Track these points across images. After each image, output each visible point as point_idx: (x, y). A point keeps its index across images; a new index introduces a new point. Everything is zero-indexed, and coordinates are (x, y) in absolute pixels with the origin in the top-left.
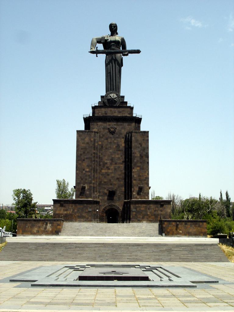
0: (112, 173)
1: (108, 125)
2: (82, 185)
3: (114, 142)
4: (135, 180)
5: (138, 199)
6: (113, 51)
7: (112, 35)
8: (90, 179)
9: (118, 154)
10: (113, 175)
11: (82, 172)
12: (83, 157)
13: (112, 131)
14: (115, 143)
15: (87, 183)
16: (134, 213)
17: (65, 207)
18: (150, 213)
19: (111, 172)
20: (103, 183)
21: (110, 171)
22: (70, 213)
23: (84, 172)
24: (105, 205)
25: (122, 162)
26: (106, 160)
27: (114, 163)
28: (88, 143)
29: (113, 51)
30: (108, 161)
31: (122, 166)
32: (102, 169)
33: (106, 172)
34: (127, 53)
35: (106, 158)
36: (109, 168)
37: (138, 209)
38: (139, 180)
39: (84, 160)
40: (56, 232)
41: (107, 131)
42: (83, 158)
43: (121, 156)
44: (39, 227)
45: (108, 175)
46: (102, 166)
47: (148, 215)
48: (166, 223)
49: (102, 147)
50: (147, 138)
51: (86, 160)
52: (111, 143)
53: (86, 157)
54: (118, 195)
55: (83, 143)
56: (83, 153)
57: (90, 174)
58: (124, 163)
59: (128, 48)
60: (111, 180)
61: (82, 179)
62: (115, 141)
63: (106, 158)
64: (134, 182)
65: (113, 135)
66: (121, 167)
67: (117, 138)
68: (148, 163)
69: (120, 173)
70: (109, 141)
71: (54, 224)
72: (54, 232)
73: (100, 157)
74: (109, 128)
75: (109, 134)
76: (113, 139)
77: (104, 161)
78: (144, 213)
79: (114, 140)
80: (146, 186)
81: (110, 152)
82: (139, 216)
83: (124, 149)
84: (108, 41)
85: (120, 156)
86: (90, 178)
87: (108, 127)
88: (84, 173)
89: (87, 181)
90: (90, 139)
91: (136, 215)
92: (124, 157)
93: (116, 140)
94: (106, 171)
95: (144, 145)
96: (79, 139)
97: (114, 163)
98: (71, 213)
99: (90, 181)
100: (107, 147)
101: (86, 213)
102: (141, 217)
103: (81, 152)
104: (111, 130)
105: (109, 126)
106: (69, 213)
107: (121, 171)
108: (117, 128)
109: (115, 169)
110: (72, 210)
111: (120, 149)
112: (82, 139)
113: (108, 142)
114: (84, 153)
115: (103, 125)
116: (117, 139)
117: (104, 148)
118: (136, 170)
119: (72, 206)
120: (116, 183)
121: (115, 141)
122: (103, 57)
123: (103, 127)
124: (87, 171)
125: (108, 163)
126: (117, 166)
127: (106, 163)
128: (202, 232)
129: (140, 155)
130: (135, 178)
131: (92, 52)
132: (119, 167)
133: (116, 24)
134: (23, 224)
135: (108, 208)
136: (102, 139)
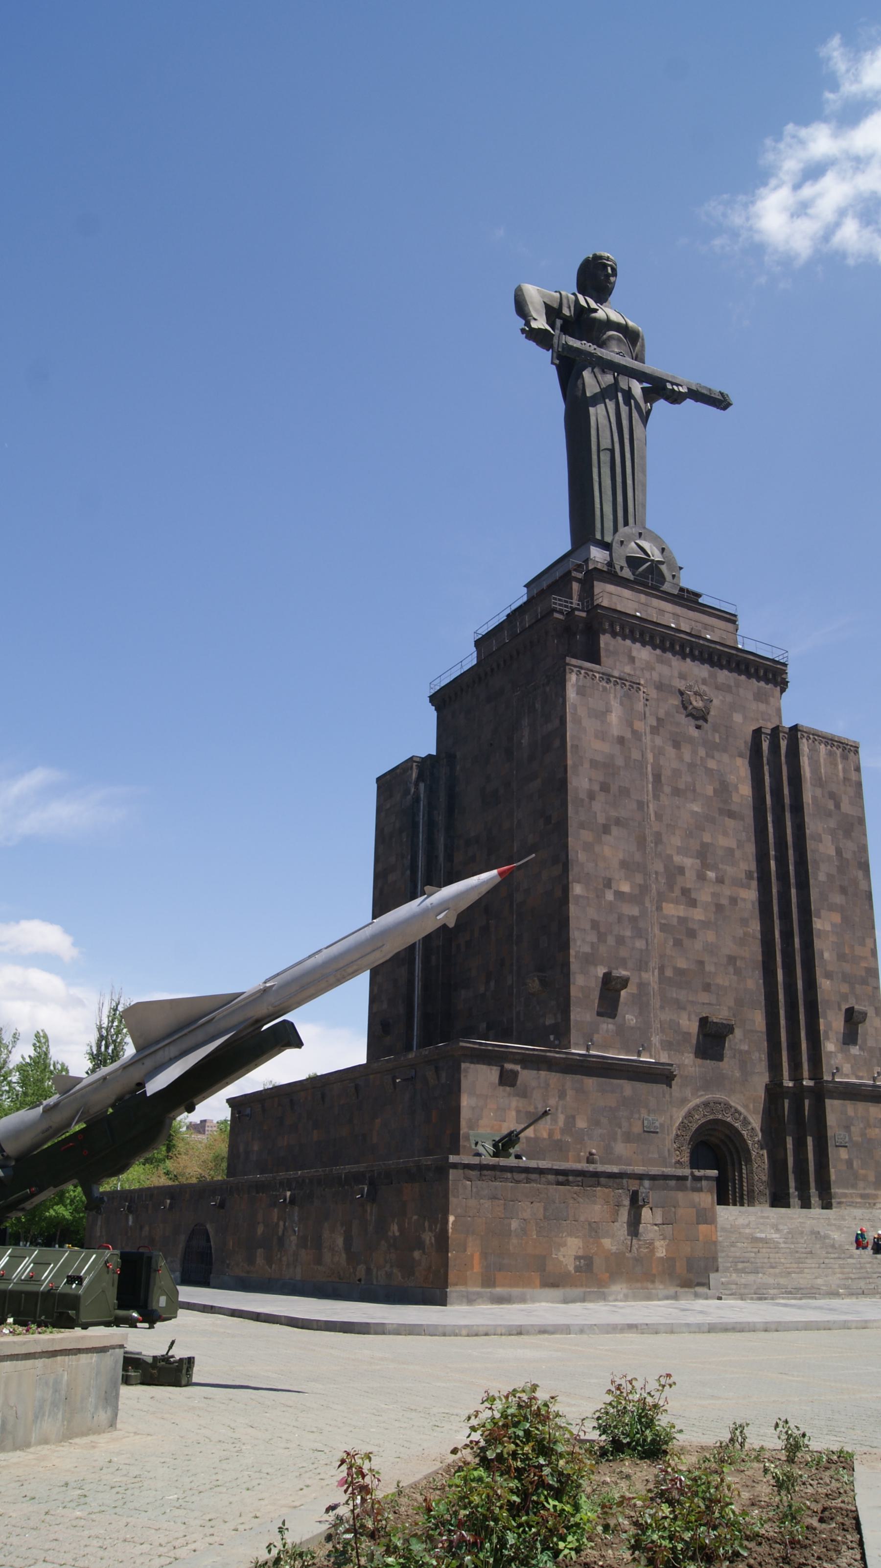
0: (705, 924)
1: (676, 674)
2: (601, 971)
3: (706, 767)
4: (828, 975)
5: (847, 1076)
9: (725, 834)
10: (710, 936)
11: (600, 896)
13: (694, 708)
14: (712, 770)
15: (623, 963)
16: (844, 1154)
17: (524, 1094)
19: (703, 918)
20: (669, 973)
21: (698, 914)
22: (551, 1133)
24: (684, 1101)
25: (743, 876)
26: (679, 851)
28: (621, 740)
31: (750, 895)
32: (661, 898)
33: (682, 914)
34: (681, 389)
35: (676, 841)
36: (693, 896)
38: (846, 978)
39: (606, 829)
40: (690, 1264)
41: (676, 701)
42: (601, 819)
43: (740, 844)
44: (594, 1231)
45: (692, 934)
46: (662, 880)
50: (853, 776)
51: (615, 830)
52: (692, 766)
53: (614, 814)
54: (741, 1052)
55: (602, 735)
56: (601, 790)
57: (635, 911)
58: (754, 884)
60: (701, 963)
61: (602, 937)
62: (712, 764)
63: (679, 844)
64: (824, 985)
65: (698, 727)
66: (744, 900)
69: (740, 932)
71: (680, 1211)
72: (680, 1267)
74: (683, 688)
75: (682, 718)
76: (702, 752)
77: (670, 857)
79: (707, 755)
81: (694, 814)
82: (862, 1172)
83: (749, 813)
84: (594, 315)
85: (733, 844)
86: (641, 937)
88: (611, 902)
89: (623, 953)
90: (630, 724)
91: (849, 1163)
92: (751, 849)
93: (713, 757)
95: (846, 807)
97: (711, 875)
98: (557, 1136)
99: (641, 950)
100: (682, 786)
101: (628, 1138)
103: (590, 780)
104: (691, 704)
105: (683, 682)
106: (545, 1135)
108: (716, 702)
109: (719, 908)
110: (561, 1119)
111: (734, 808)
113: (680, 759)
115: (653, 669)
116: (717, 755)
117: (667, 789)
118: (828, 927)
119: (562, 1095)
120: (727, 984)
123: (655, 676)
124: (623, 893)
125: (687, 874)
127: (681, 870)
129: (839, 852)
130: (830, 968)
132: (734, 901)
134: (487, 1204)
135: (700, 1119)
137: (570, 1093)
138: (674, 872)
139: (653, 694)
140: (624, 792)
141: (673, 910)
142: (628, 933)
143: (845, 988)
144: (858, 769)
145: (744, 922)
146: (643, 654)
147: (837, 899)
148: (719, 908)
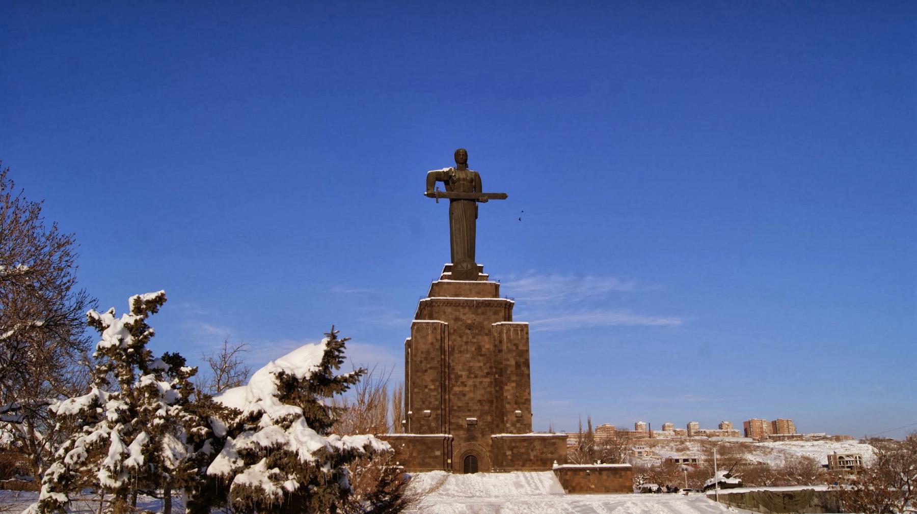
4: (509, 403)
6: (463, 194)
7: (458, 169)
8: (437, 403)
9: (479, 361)
10: (471, 395)
11: (423, 391)
12: (424, 366)
18: (535, 456)
21: (467, 389)
23: (427, 390)
27: (473, 376)
28: (432, 344)
29: (463, 194)
30: (463, 373)
32: (453, 386)
37: (515, 451)
38: (516, 403)
39: (426, 371)
43: (485, 364)
45: (464, 395)
47: (531, 460)
48: (569, 473)
49: (453, 349)
50: (525, 336)
51: (429, 371)
52: (467, 343)
53: (429, 366)
59: (487, 188)
61: (423, 403)
62: (475, 340)
64: (508, 406)
67: (477, 334)
68: (529, 375)
69: (482, 392)
70: (465, 340)
73: (449, 367)
76: (470, 337)
78: (525, 457)
80: (526, 412)
85: (482, 364)
87: (462, 316)
89: (431, 406)
91: (511, 460)
92: (488, 365)
94: (461, 389)
95: (521, 347)
96: (418, 337)
97: (473, 376)
100: (462, 349)
101: (430, 457)
102: (521, 463)
107: (485, 389)
109: (475, 386)
112: (423, 337)
114: (426, 359)
121: (475, 340)
122: (446, 202)
126: (478, 380)
127: (461, 376)
128: (625, 487)
131: (428, 195)
133: (466, 152)
135: (463, 450)
136: (453, 337)
137: (411, 447)
138: (458, 377)
139: (452, 322)
140: (433, 359)
141: (456, 389)
142: (433, 400)
143: (515, 406)
144: (527, 333)
145: (485, 389)
146: (449, 310)
147: (514, 378)
148: (475, 386)
